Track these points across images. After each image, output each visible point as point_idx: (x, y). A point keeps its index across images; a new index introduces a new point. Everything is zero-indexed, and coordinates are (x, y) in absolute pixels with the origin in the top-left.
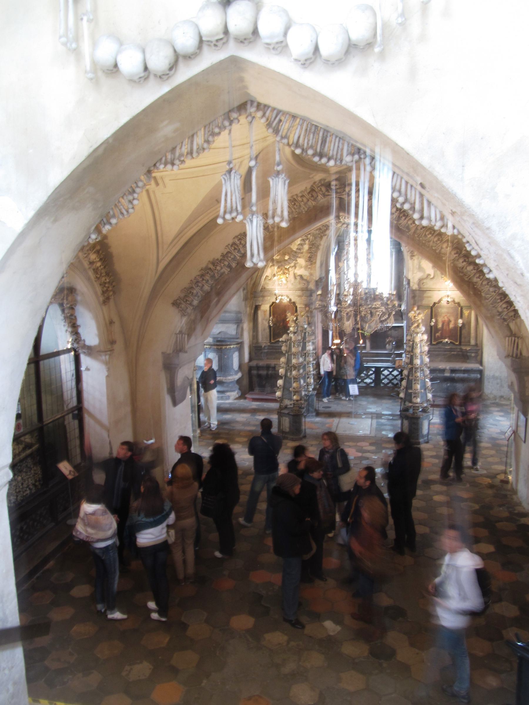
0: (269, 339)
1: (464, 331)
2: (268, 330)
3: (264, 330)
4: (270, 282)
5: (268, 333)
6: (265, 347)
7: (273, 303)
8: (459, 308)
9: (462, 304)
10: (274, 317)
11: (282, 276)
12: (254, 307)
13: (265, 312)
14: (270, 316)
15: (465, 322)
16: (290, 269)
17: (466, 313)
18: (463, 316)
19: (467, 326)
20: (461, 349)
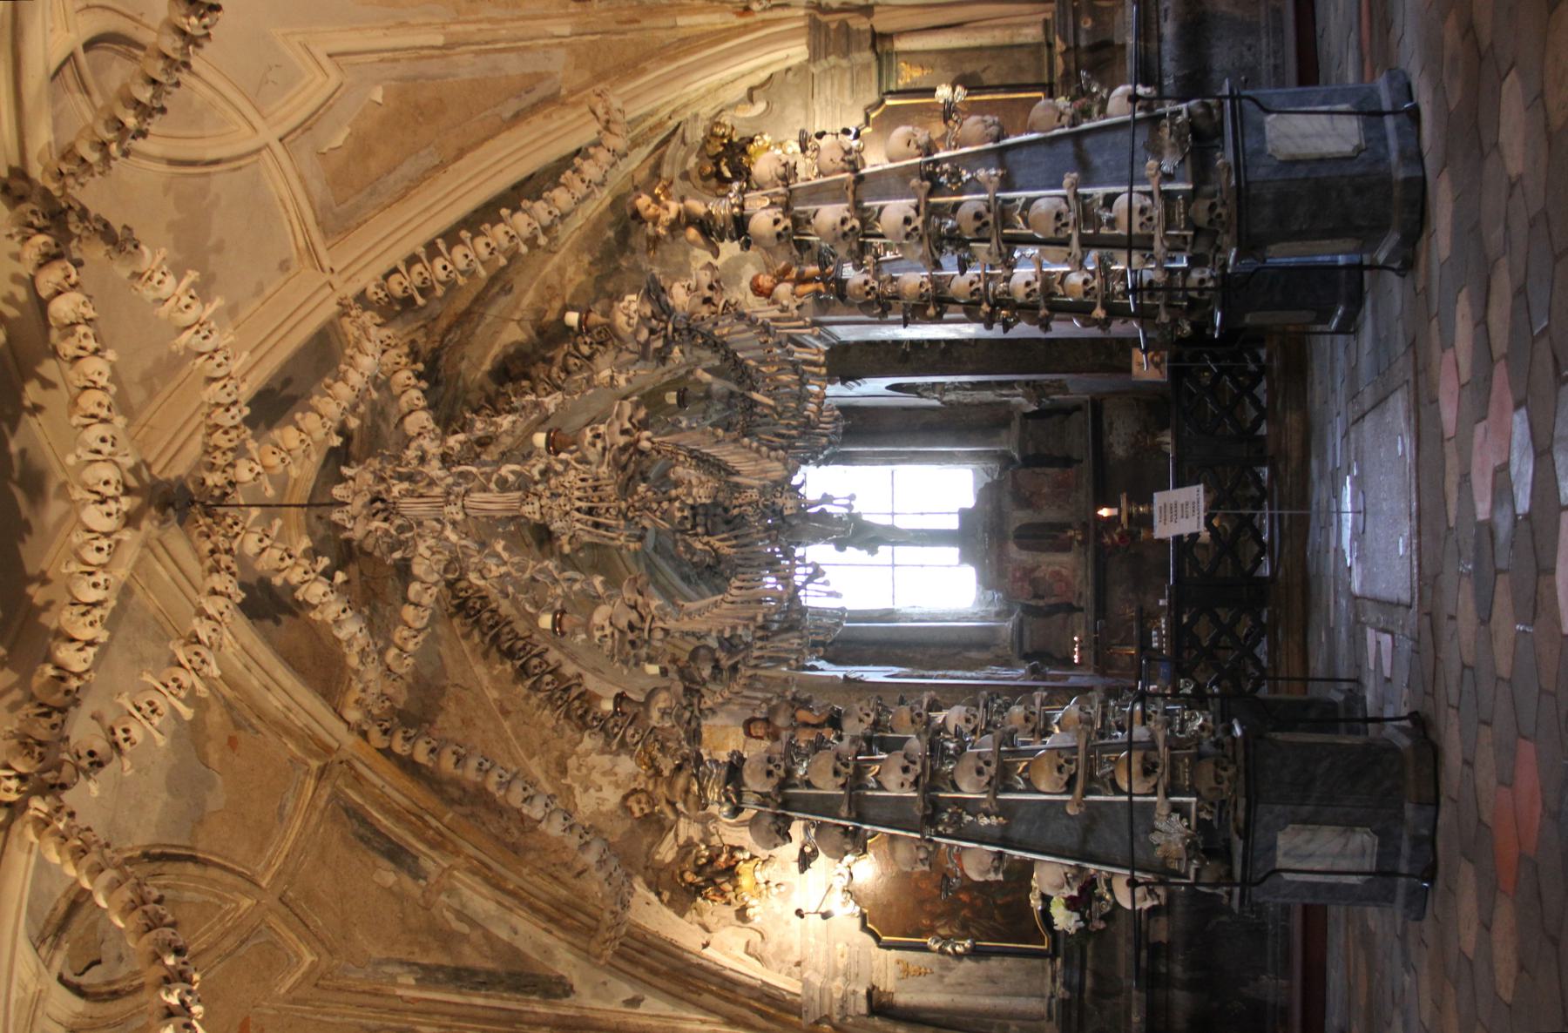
0: (1037, 962)
1: (989, 78)
2: (994, 963)
3: (992, 980)
4: (774, 936)
5: (1009, 962)
6: (1067, 985)
7: (864, 927)
8: (889, 102)
9: (873, 97)
10: (930, 931)
11: (745, 881)
12: (877, 1021)
13: (906, 972)
14: (924, 948)
15: (951, 76)
16: (715, 841)
17: (909, 75)
18: (924, 85)
19: (968, 68)
20: (1066, 73)
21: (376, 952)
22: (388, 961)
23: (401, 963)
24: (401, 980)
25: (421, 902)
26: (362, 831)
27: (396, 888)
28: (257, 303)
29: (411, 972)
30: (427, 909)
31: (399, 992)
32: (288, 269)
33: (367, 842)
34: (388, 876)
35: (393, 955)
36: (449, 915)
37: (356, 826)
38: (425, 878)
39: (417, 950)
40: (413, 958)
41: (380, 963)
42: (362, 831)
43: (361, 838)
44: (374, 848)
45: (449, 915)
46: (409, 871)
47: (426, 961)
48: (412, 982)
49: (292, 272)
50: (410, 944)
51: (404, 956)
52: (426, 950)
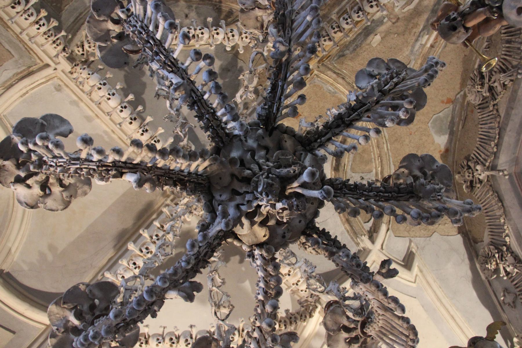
21: (407, 52)
22: (413, 46)
23: (417, 40)
24: (423, 43)
25: (394, 21)
26: (351, 49)
27: (383, 35)
28: (82, 104)
29: (423, 37)
30: (398, 19)
31: (428, 45)
32: (59, 85)
33: (357, 46)
34: (376, 39)
35: (411, 43)
36: (406, 10)
37: (347, 52)
38: (384, 18)
39: (414, 30)
40: (417, 34)
41: (412, 51)
42: (351, 49)
43: (355, 50)
44: (361, 44)
45: (406, 10)
46: (378, 26)
47: (421, 27)
48: (427, 36)
49: (61, 83)
50: (410, 33)
51: (414, 38)
52: (416, 25)
